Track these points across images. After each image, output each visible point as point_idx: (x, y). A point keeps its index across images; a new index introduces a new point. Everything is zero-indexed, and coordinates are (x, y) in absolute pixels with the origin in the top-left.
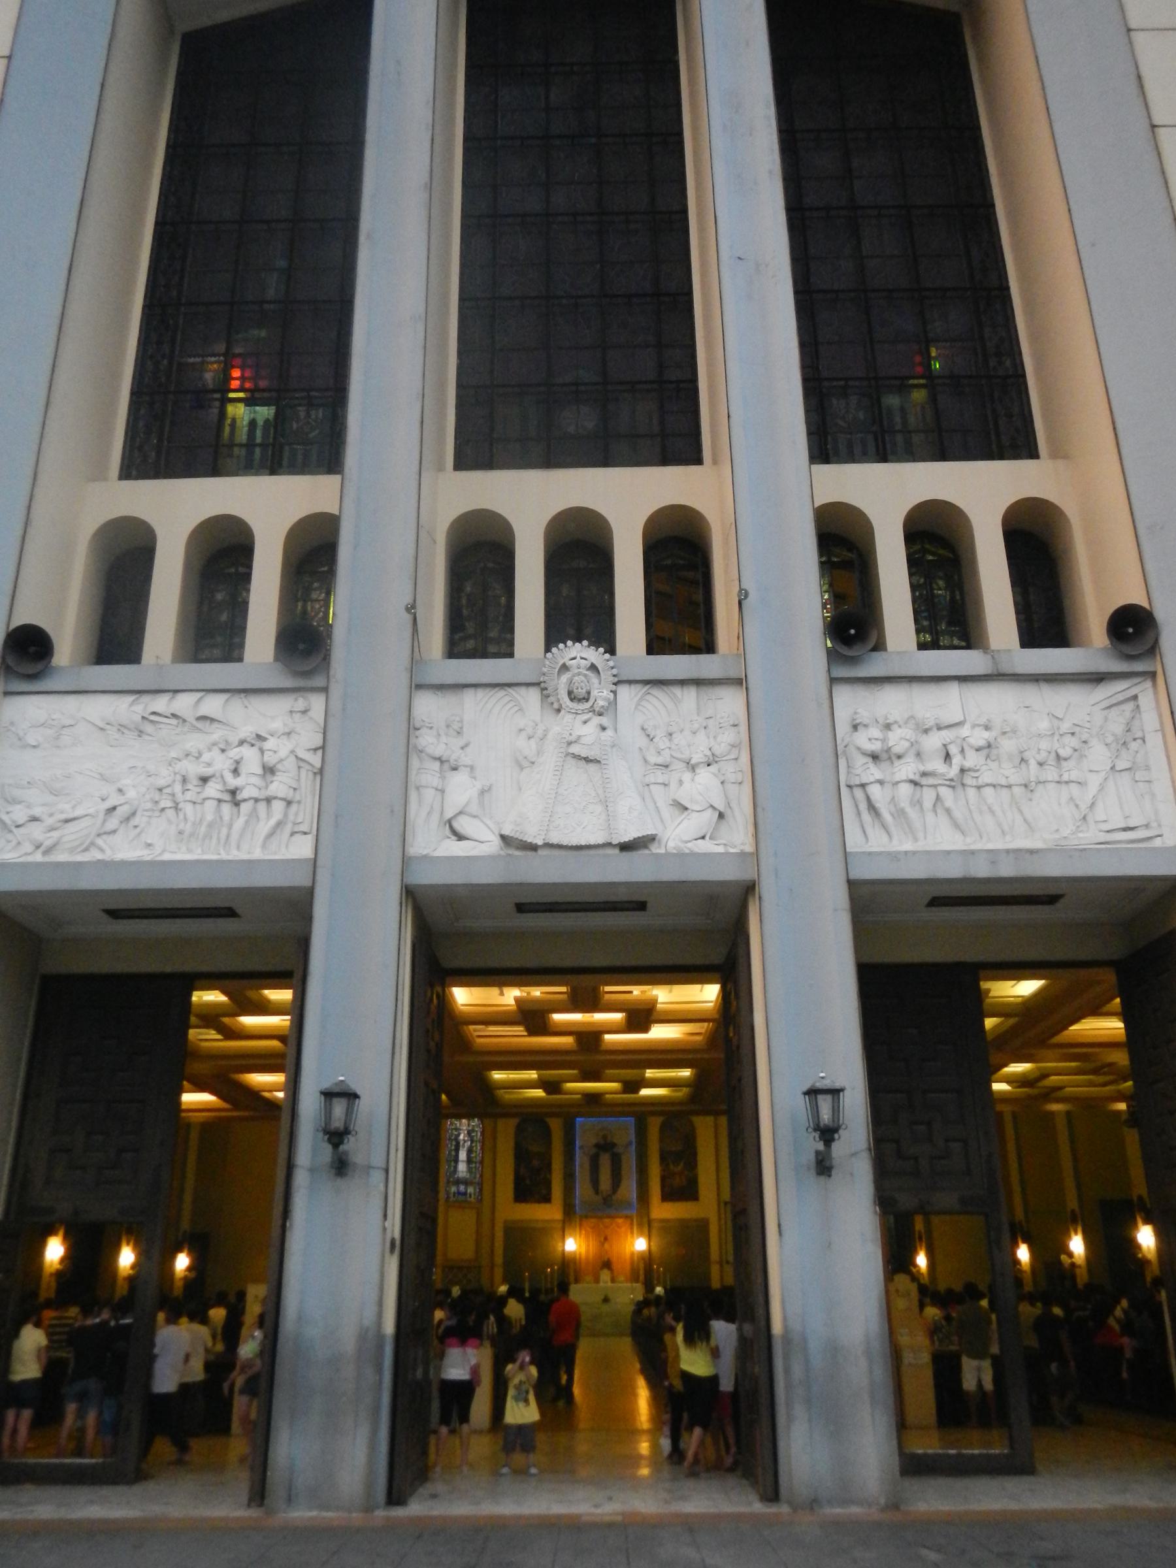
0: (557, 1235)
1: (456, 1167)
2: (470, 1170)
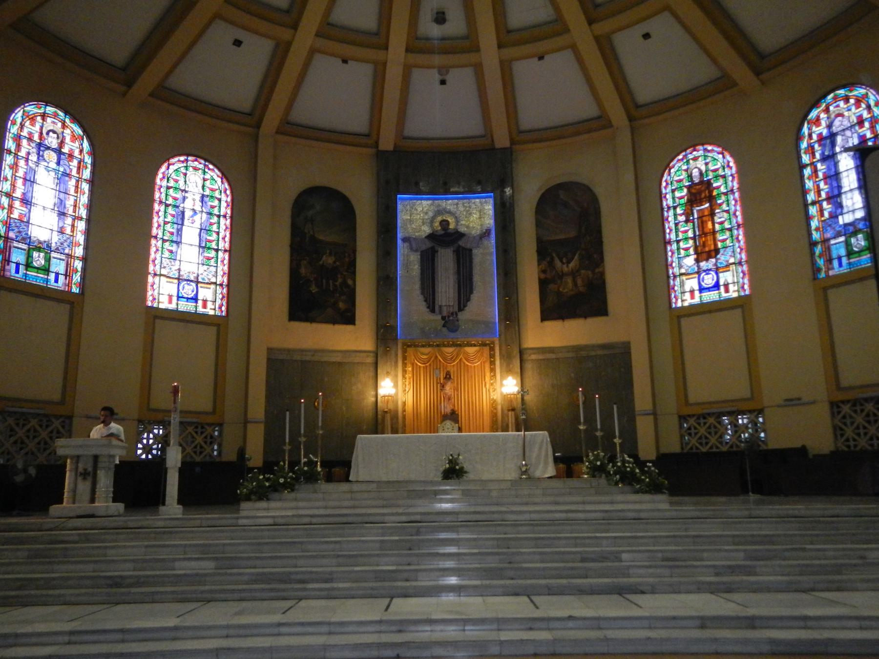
0: (365, 376)
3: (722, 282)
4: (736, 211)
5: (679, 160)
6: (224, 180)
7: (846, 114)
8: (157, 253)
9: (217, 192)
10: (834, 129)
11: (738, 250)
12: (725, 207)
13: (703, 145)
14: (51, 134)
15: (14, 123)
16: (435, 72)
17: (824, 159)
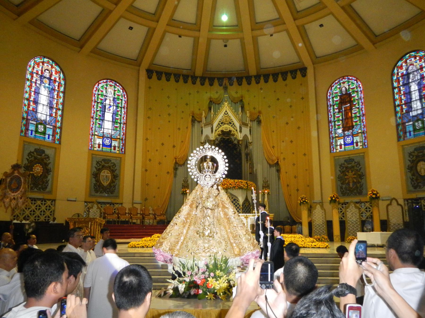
2: (115, 128)
3: (355, 141)
4: (362, 108)
5: (336, 83)
6: (124, 91)
7: (415, 64)
8: (94, 125)
9: (121, 96)
10: (409, 71)
11: (363, 126)
12: (357, 106)
13: (347, 76)
14: (46, 71)
15: (30, 66)
16: (221, 41)
17: (404, 85)
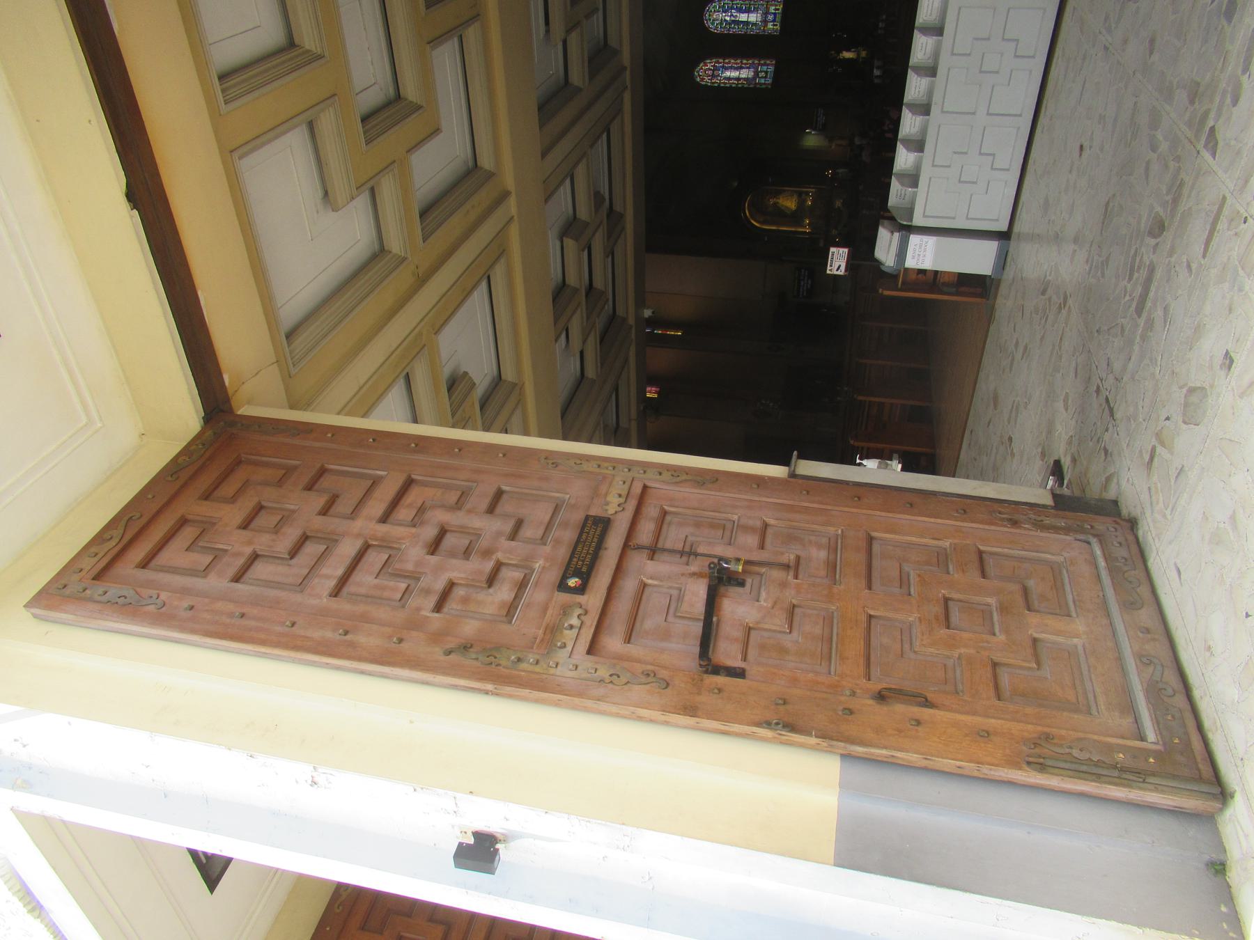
1: (753, 24)
2: (756, 10)
